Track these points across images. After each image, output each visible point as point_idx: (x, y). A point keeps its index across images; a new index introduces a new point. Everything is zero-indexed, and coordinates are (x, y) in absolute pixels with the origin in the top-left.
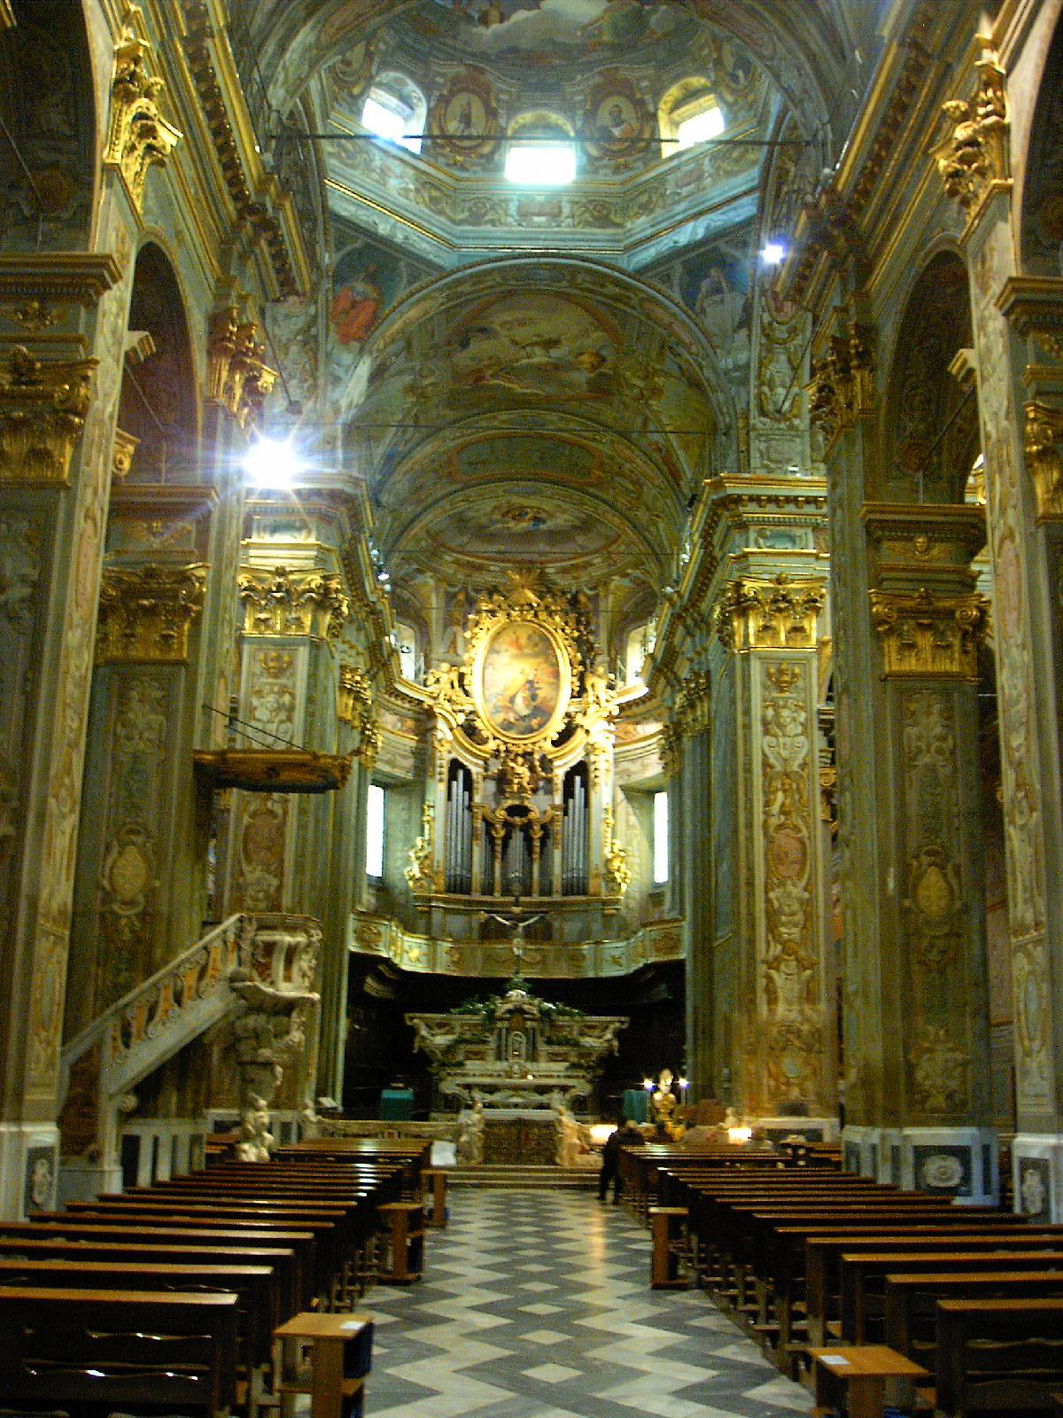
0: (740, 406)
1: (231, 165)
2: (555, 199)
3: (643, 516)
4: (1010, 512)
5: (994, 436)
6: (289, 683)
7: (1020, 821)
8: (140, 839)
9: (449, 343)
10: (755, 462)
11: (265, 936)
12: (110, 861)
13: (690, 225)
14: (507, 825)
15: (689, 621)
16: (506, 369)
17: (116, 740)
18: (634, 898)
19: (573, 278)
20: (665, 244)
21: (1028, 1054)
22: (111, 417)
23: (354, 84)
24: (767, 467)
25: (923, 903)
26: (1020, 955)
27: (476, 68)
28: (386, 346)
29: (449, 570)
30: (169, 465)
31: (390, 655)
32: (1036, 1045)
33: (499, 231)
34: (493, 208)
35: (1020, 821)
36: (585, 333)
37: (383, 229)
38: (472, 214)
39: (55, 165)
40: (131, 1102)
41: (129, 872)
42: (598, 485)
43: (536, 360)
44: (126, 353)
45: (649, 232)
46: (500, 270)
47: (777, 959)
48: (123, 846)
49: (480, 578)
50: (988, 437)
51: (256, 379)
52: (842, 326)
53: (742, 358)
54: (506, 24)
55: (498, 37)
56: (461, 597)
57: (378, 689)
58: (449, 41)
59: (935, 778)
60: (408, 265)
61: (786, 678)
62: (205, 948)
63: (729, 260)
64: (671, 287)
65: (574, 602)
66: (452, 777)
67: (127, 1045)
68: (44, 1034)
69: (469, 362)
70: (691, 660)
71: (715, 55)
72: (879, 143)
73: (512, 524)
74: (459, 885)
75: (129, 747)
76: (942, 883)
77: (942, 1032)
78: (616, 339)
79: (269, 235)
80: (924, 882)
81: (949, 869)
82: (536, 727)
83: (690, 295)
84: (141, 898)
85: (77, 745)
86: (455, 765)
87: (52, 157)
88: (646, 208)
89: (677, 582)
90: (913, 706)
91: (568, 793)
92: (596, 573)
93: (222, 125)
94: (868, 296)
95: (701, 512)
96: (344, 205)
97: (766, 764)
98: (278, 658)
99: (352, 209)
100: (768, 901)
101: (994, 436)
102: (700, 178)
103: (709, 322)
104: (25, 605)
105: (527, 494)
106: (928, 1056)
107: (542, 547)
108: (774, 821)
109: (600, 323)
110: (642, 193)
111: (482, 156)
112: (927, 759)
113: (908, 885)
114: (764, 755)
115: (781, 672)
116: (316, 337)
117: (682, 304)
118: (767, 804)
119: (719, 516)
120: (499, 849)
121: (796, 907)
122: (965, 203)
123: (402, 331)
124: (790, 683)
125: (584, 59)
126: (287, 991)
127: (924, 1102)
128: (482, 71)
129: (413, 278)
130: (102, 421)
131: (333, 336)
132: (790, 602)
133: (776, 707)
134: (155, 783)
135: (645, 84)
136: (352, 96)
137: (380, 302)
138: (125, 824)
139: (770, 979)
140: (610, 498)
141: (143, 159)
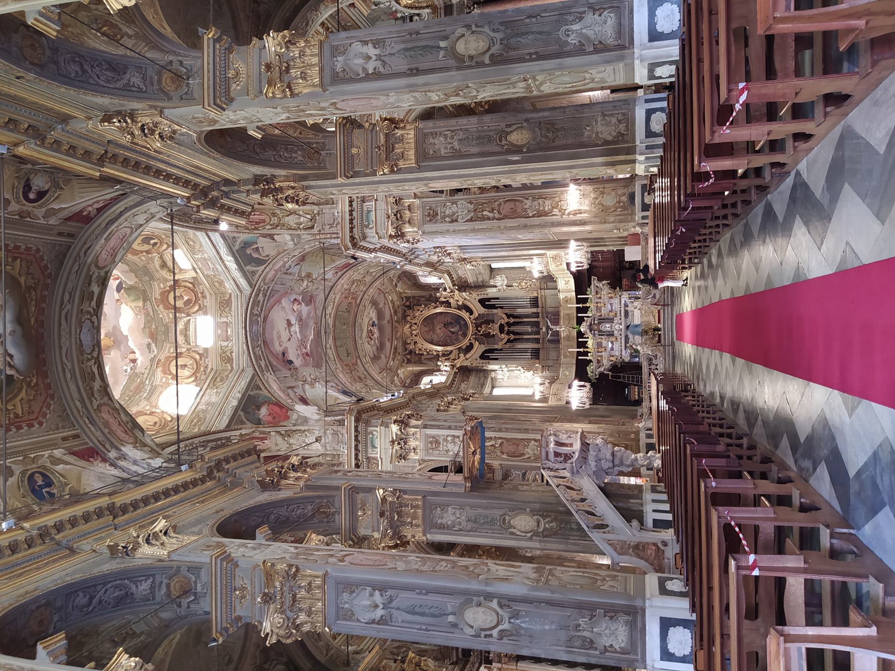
0: (309, 237)
1: (185, 486)
2: (218, 325)
3: (368, 279)
4: (323, 105)
5: (287, 115)
6: (442, 438)
7: (475, 93)
8: (507, 518)
9: (290, 369)
10: (334, 230)
11: (551, 456)
12: (519, 533)
13: (227, 263)
14: (508, 333)
15: (412, 257)
16: (302, 343)
17: (461, 530)
19: (256, 315)
20: (237, 275)
21: (593, 80)
22: (296, 548)
23: (166, 420)
24: (337, 225)
25: (525, 142)
26: (542, 88)
27: (158, 364)
28: (290, 398)
30: (331, 507)
31: (434, 388)
32: (587, 76)
33: (235, 349)
34: (224, 353)
35: (475, 93)
36: (283, 308)
37: (235, 403)
38: (228, 362)
39: (168, 586)
40: (635, 523)
41: (523, 523)
42: (355, 299)
43: (298, 331)
44: (266, 540)
45: (232, 282)
46: (253, 348)
47: (560, 211)
48: (511, 527)
49: (400, 350)
50: (288, 118)
51: (293, 466)
52: (255, 192)
53: (288, 238)
54: (136, 350)
55: (142, 354)
56: (409, 357)
57: (448, 393)
58: (145, 376)
59: (465, 139)
60: (251, 391)
61: (431, 213)
62: (558, 487)
63: (243, 245)
64: (257, 271)
65: (409, 307)
66: (488, 358)
67: (607, 526)
68: (599, 583)
69: (300, 359)
70: (429, 255)
71: (145, 254)
72: (159, 176)
73: (375, 336)
74: (536, 354)
75: (464, 524)
76: (515, 133)
77: (588, 128)
78: (286, 294)
79: (224, 463)
80: (515, 142)
81: (508, 130)
83: (260, 262)
84: (535, 517)
85: (454, 562)
86: (483, 357)
87: (164, 586)
88: (221, 283)
89: (394, 263)
90: (431, 152)
91: (493, 307)
92: (395, 298)
93: (163, 493)
94: (239, 180)
95: (359, 254)
96: (223, 421)
97: (471, 220)
98: (431, 443)
99: (225, 417)
100: (533, 216)
101: (287, 115)
102: (205, 260)
103: (273, 253)
104: (384, 594)
105: (362, 330)
106: (600, 135)
107: (385, 322)
108: (497, 215)
109: (279, 301)
110: (214, 286)
111: (201, 359)
112: (456, 143)
113: (516, 149)
114: (467, 221)
115: (429, 215)
116: (286, 431)
117: (265, 266)
118: (489, 219)
119: (360, 246)
120: (520, 337)
121: (536, 203)
122: (174, 132)
123: (284, 391)
124: (434, 211)
125: (151, 314)
126: (577, 446)
127: (622, 135)
128: (159, 360)
129: (259, 388)
130: (297, 553)
131: (284, 424)
132: (397, 212)
133: (444, 217)
134: (480, 511)
135: (161, 285)
136: (171, 421)
137: (268, 402)
138: (500, 525)
139: (569, 214)
140: (362, 294)
141: (170, 537)
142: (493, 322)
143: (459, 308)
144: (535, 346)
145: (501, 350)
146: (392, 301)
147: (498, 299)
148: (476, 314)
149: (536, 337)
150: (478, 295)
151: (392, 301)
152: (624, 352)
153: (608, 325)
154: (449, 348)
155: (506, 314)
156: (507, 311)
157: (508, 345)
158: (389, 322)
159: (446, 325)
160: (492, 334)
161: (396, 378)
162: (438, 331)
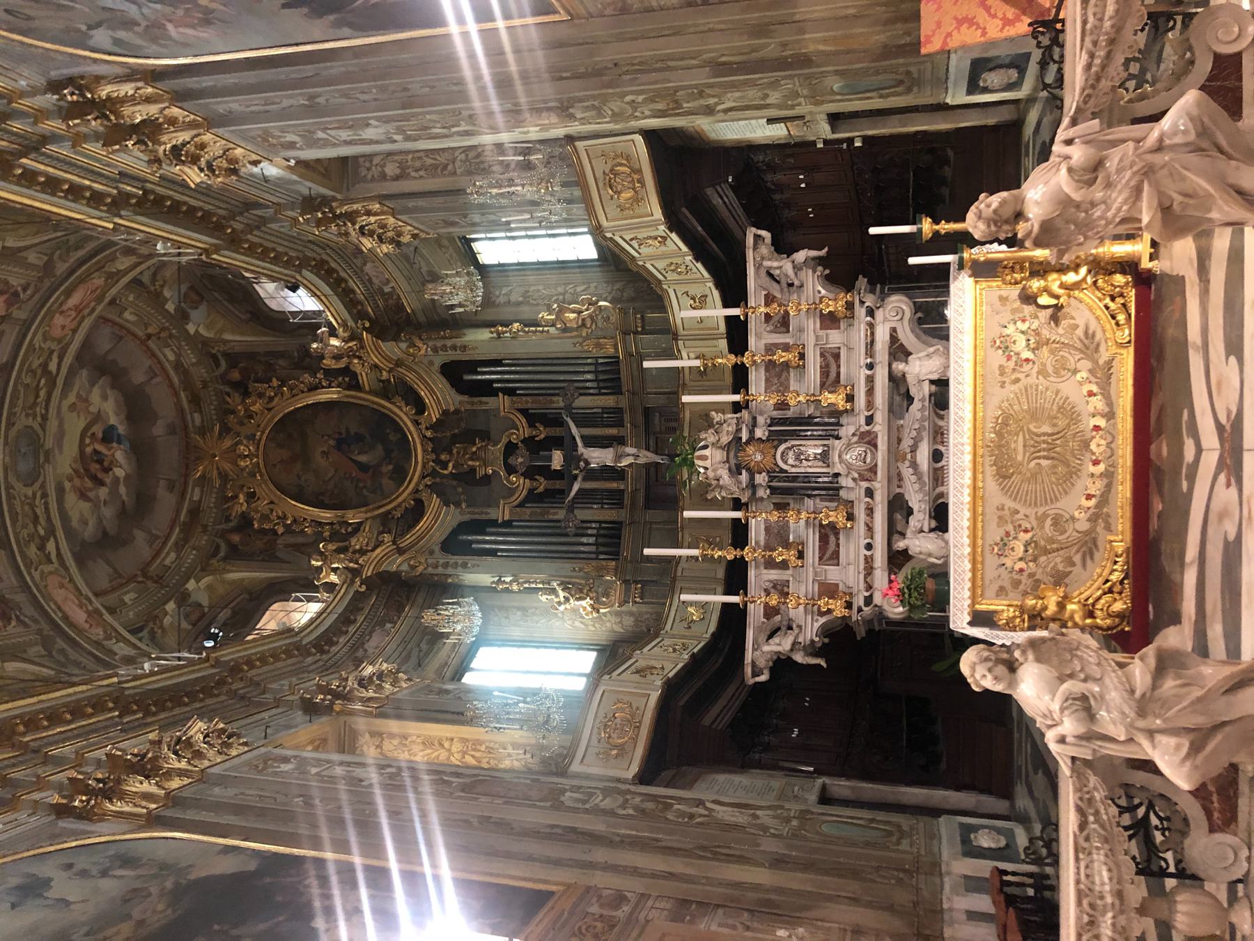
18: (622, 291)
29: (191, 556)
56: (236, 538)
66: (467, 550)
73: (120, 472)
82: (399, 436)
91: (487, 389)
92: (190, 358)
107: (159, 430)
142: (486, 436)
143: (385, 390)
144: (609, 514)
145: (508, 524)
146: (178, 366)
147: (498, 362)
148: (434, 414)
149: (614, 485)
150: (435, 350)
151: (178, 366)
152: (880, 578)
153: (813, 449)
154: (353, 517)
155: (524, 412)
156: (527, 403)
157: (527, 512)
158: (172, 430)
159: (343, 444)
160: (480, 473)
161: (171, 606)
162: (321, 461)
